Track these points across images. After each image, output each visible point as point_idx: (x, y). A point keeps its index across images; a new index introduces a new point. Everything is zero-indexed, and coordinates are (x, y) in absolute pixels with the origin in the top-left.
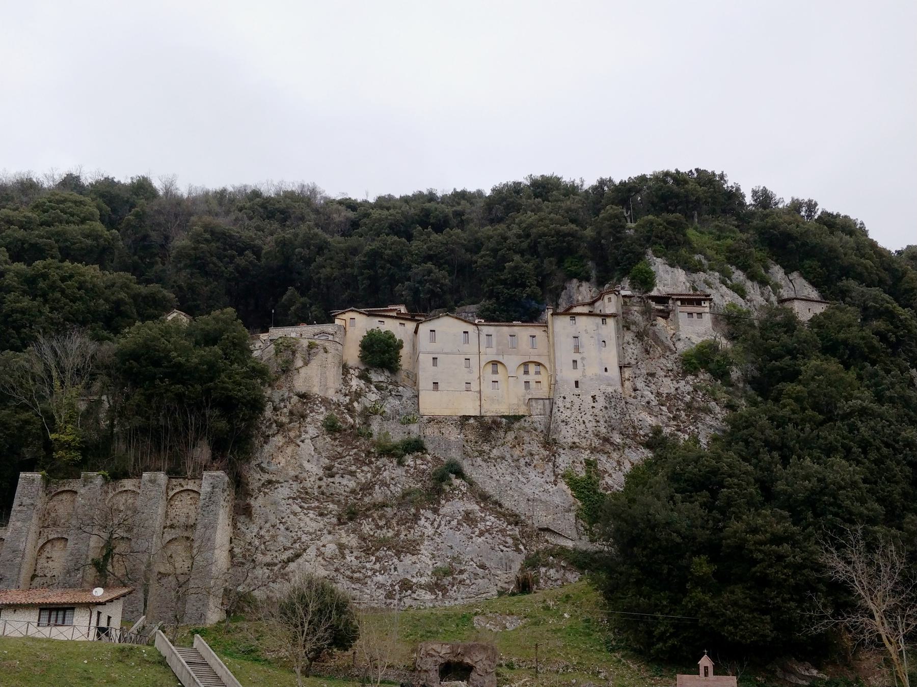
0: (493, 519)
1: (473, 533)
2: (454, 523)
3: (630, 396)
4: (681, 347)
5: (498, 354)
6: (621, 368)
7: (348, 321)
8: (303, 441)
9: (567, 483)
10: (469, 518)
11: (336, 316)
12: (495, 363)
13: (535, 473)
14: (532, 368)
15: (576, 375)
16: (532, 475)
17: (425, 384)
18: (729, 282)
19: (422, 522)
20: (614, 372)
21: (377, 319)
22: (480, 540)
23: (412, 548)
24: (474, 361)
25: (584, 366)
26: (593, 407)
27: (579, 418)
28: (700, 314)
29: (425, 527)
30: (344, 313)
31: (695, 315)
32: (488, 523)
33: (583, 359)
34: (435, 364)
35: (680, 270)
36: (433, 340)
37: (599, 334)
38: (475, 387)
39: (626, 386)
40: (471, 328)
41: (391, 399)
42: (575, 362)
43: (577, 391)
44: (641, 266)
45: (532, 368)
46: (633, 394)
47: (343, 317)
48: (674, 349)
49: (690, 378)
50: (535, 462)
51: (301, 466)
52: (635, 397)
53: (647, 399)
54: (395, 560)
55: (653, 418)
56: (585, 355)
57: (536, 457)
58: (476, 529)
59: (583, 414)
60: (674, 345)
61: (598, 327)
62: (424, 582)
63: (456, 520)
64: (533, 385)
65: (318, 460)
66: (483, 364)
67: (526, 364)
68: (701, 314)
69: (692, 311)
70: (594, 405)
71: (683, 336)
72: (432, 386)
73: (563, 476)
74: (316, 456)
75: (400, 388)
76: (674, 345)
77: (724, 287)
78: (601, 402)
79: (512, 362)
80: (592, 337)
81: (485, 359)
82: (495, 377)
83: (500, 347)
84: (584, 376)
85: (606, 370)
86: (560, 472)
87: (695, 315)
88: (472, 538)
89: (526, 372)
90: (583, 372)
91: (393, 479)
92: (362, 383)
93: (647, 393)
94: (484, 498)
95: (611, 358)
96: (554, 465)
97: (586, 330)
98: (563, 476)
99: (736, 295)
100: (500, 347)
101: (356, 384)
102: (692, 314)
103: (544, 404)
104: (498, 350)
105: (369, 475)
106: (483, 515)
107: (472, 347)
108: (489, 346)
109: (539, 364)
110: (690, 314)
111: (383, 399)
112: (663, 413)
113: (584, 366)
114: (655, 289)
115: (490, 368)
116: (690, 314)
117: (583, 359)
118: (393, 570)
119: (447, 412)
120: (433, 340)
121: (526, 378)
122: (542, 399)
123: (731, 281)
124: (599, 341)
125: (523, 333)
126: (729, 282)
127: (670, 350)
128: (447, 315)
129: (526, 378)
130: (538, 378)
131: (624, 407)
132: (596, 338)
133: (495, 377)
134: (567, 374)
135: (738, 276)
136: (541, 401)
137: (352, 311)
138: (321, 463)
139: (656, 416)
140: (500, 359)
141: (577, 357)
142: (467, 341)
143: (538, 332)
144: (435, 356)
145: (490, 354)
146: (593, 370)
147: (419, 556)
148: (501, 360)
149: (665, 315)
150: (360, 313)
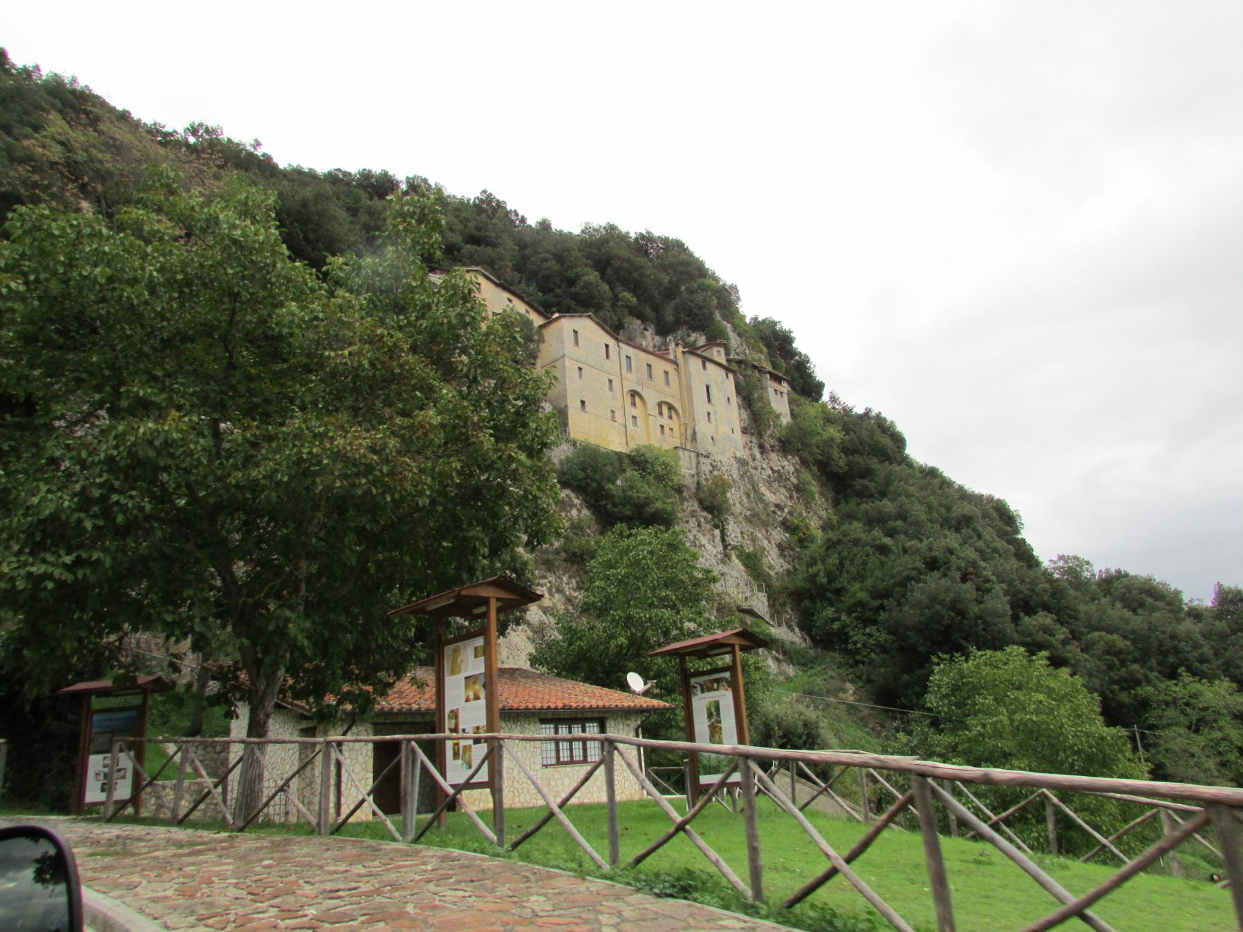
5: (638, 384)
12: (634, 394)
24: (616, 384)
38: (618, 415)
40: (611, 342)
42: (709, 414)
64: (666, 430)
79: (652, 399)
89: (661, 413)
108: (630, 368)
109: (671, 408)
115: (628, 400)
128: (589, 317)
133: (634, 412)
134: (704, 429)
141: (709, 408)
148: (642, 393)
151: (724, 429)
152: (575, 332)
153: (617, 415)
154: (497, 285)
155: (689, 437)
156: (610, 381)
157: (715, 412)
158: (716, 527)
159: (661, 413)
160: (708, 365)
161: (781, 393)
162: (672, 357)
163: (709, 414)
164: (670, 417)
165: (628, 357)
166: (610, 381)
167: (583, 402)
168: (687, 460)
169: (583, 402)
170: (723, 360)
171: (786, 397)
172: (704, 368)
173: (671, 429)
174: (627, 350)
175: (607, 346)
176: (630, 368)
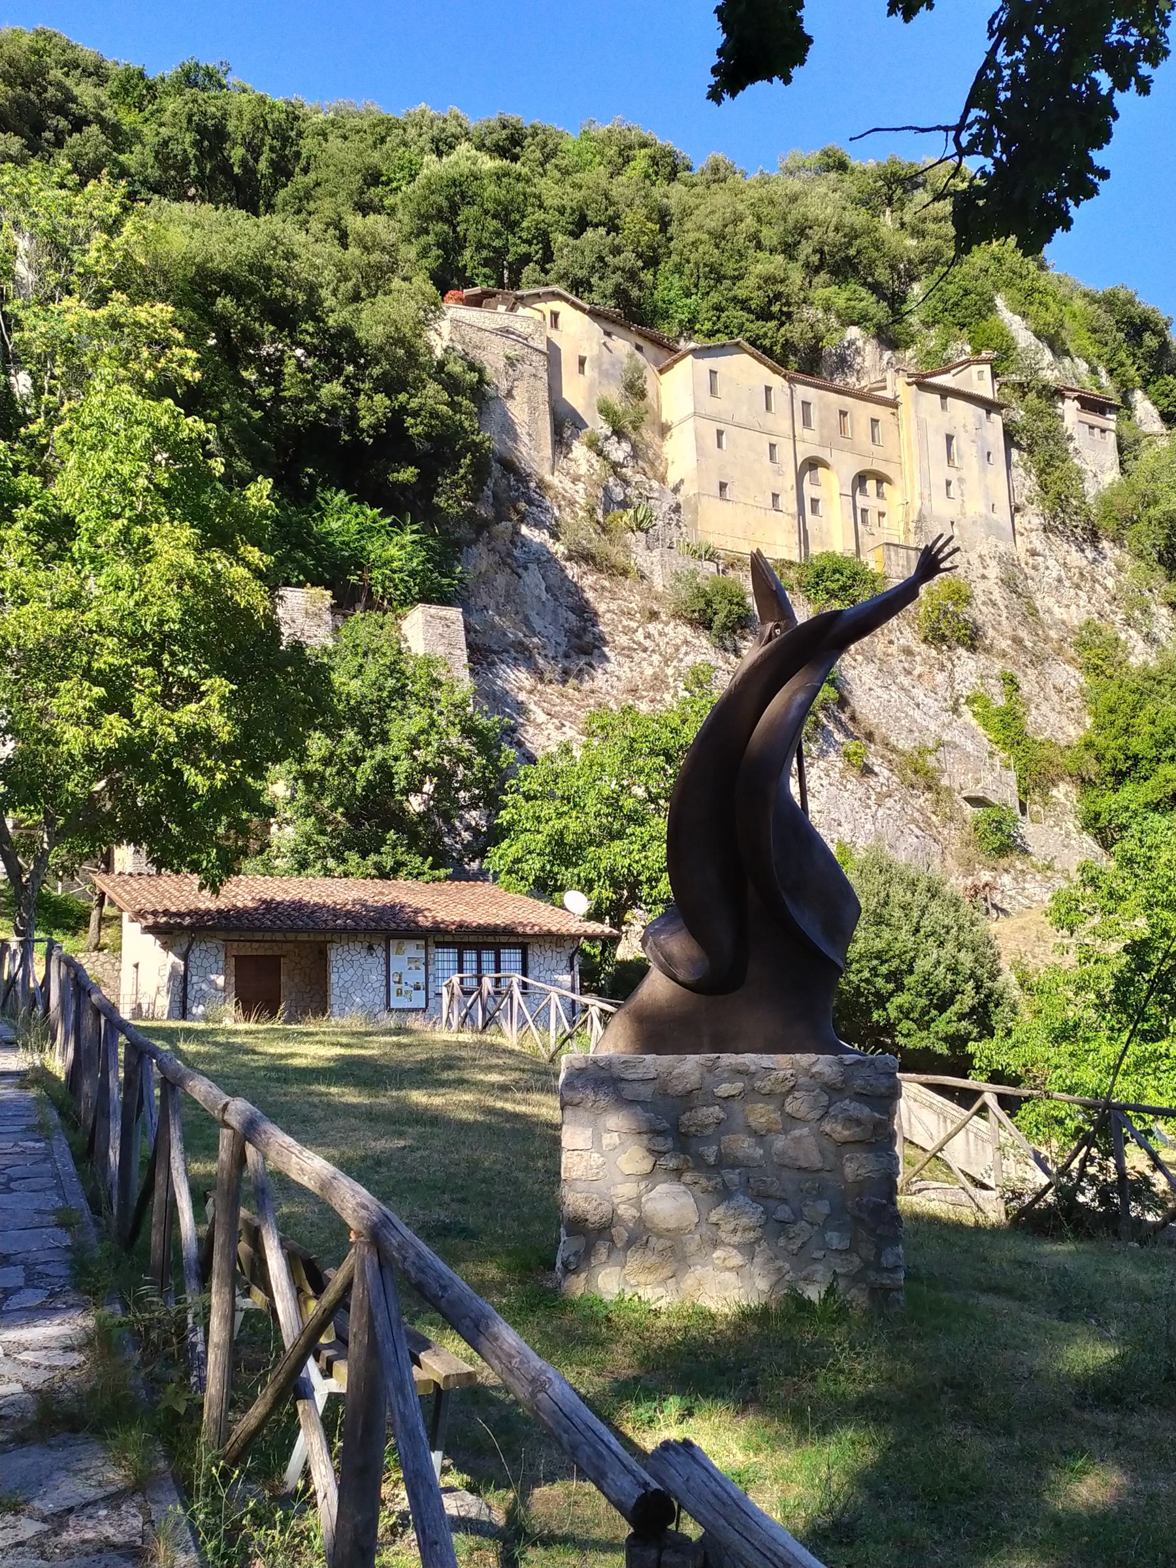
0: (886, 773)
2: (835, 775)
8: (526, 568)
9: (975, 714)
12: (813, 464)
24: (785, 451)
28: (1103, 431)
31: (1097, 431)
34: (719, 445)
40: (778, 382)
42: (948, 483)
45: (871, 485)
46: (1030, 561)
51: (527, 621)
52: (1035, 568)
53: (1055, 574)
55: (1062, 610)
56: (964, 473)
64: (872, 517)
65: (555, 612)
70: (986, 572)
73: (970, 701)
74: (551, 605)
81: (806, 451)
84: (964, 514)
87: (1097, 431)
89: (864, 492)
93: (1051, 562)
98: (970, 701)
103: (908, 558)
104: (821, 437)
105: (656, 658)
107: (780, 421)
108: (807, 423)
109: (881, 479)
110: (1092, 427)
112: (1082, 603)
116: (1092, 427)
122: (907, 548)
130: (881, 505)
136: (902, 552)
138: (562, 621)
139: (1068, 606)
140: (823, 454)
141: (952, 475)
144: (722, 427)
146: (976, 507)
150: (574, 305)
152: (713, 373)
155: (912, 526)
156: (772, 446)
157: (961, 480)
158: (942, 668)
161: (1103, 431)
162: (887, 394)
163: (948, 483)
164: (880, 495)
165: (806, 405)
166: (772, 446)
167: (723, 486)
168: (902, 562)
169: (723, 486)
170: (986, 388)
171: (1111, 438)
172: (944, 407)
173: (881, 514)
174: (804, 392)
175: (768, 389)
176: (807, 423)
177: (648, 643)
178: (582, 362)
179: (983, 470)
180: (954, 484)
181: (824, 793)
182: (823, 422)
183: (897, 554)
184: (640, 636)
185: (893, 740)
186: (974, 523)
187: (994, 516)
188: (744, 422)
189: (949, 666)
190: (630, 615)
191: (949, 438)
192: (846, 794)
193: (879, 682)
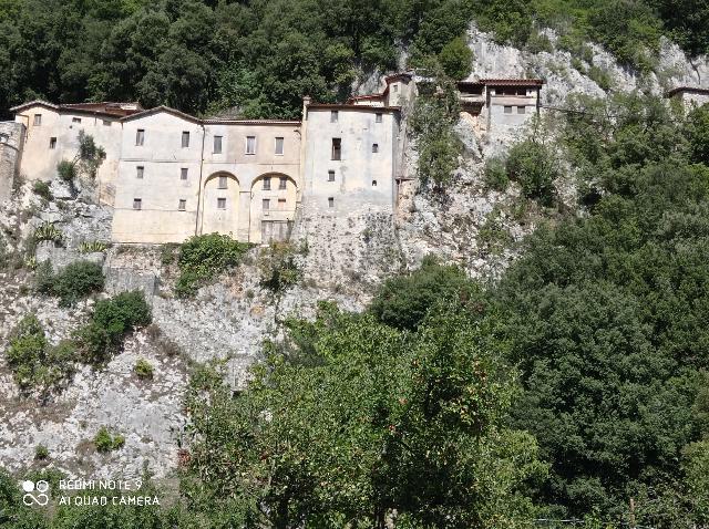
1: (142, 396)
2: (118, 382)
3: (405, 219)
4: (489, 152)
6: (398, 182)
7: (32, 118)
10: (144, 374)
11: (16, 112)
13: (249, 319)
14: (275, 182)
15: (332, 189)
16: (244, 323)
17: (124, 199)
18: (585, 66)
19: (78, 378)
20: (386, 185)
21: (71, 117)
22: (150, 405)
23: (59, 414)
24: (193, 173)
25: (344, 180)
26: (347, 233)
27: (326, 247)
29: (81, 388)
30: (26, 108)
32: (167, 384)
33: (343, 169)
35: (512, 49)
36: (140, 141)
37: (369, 135)
38: (191, 205)
39: (401, 205)
40: (193, 127)
41: (76, 221)
42: (332, 173)
43: (330, 212)
44: (455, 44)
45: (275, 182)
46: (409, 216)
47: (26, 113)
48: (480, 157)
49: (492, 194)
50: (253, 305)
54: (33, 429)
57: (255, 299)
58: (148, 392)
59: (332, 242)
60: (480, 150)
61: (369, 125)
62: (65, 458)
63: (122, 379)
64: (274, 204)
66: (206, 175)
67: (267, 177)
68: (523, 107)
69: (506, 103)
70: (350, 230)
71: (493, 138)
72: (131, 203)
73: (288, 324)
75: (92, 207)
76: (480, 150)
77: (576, 72)
78: (361, 226)
79: (247, 172)
80: (359, 139)
81: (208, 170)
82: (222, 194)
83: (232, 153)
85: (374, 182)
86: (283, 319)
88: (139, 402)
89: (267, 187)
90: (342, 186)
91: (50, 324)
92: (37, 199)
94: (171, 351)
95: (383, 165)
96: (277, 308)
97: (351, 129)
99: (593, 84)
100: (232, 153)
101: (29, 198)
102: (510, 106)
103: (281, 228)
104: (229, 157)
106: (163, 373)
108: (218, 148)
109: (284, 178)
110: (508, 107)
111: (66, 221)
113: (344, 180)
114: (472, 75)
117: (343, 169)
118: (27, 442)
119: (150, 239)
120: (140, 141)
121: (266, 194)
123: (591, 65)
124: (368, 144)
125: (266, 134)
126: (585, 66)
127: (475, 158)
128: (163, 110)
129: (266, 194)
130: (282, 194)
131: (393, 234)
132: (365, 140)
135: (602, 58)
137: (39, 105)
141: (335, 165)
142: (186, 143)
143: (286, 132)
144: (141, 164)
145: (218, 162)
147: (65, 424)
149: (474, 109)
151: (356, 183)
153: (187, 204)
154: (57, 110)
156: (184, 171)
159: (267, 187)
160: (340, 113)
163: (332, 173)
164: (283, 187)
165: (218, 138)
166: (184, 171)
174: (214, 130)
176: (218, 148)
177: (18, 310)
178: (53, 140)
179: (368, 158)
180: (337, 175)
181: (106, 394)
182: (231, 148)
183: (271, 227)
184: (13, 306)
185: (193, 357)
186: (352, 196)
187: (374, 187)
188: (161, 157)
189: (276, 301)
190: (11, 293)
191: (337, 143)
192: (122, 395)
193: (212, 318)
